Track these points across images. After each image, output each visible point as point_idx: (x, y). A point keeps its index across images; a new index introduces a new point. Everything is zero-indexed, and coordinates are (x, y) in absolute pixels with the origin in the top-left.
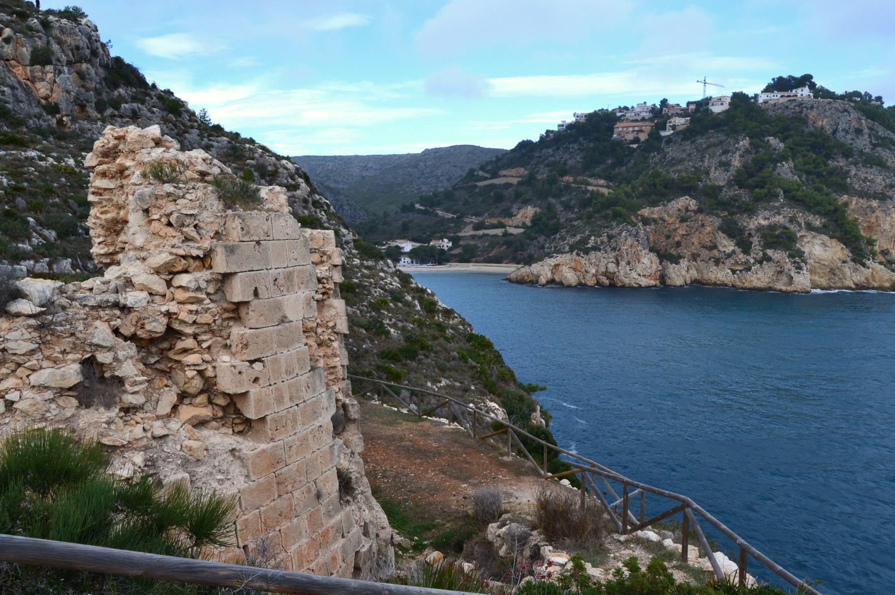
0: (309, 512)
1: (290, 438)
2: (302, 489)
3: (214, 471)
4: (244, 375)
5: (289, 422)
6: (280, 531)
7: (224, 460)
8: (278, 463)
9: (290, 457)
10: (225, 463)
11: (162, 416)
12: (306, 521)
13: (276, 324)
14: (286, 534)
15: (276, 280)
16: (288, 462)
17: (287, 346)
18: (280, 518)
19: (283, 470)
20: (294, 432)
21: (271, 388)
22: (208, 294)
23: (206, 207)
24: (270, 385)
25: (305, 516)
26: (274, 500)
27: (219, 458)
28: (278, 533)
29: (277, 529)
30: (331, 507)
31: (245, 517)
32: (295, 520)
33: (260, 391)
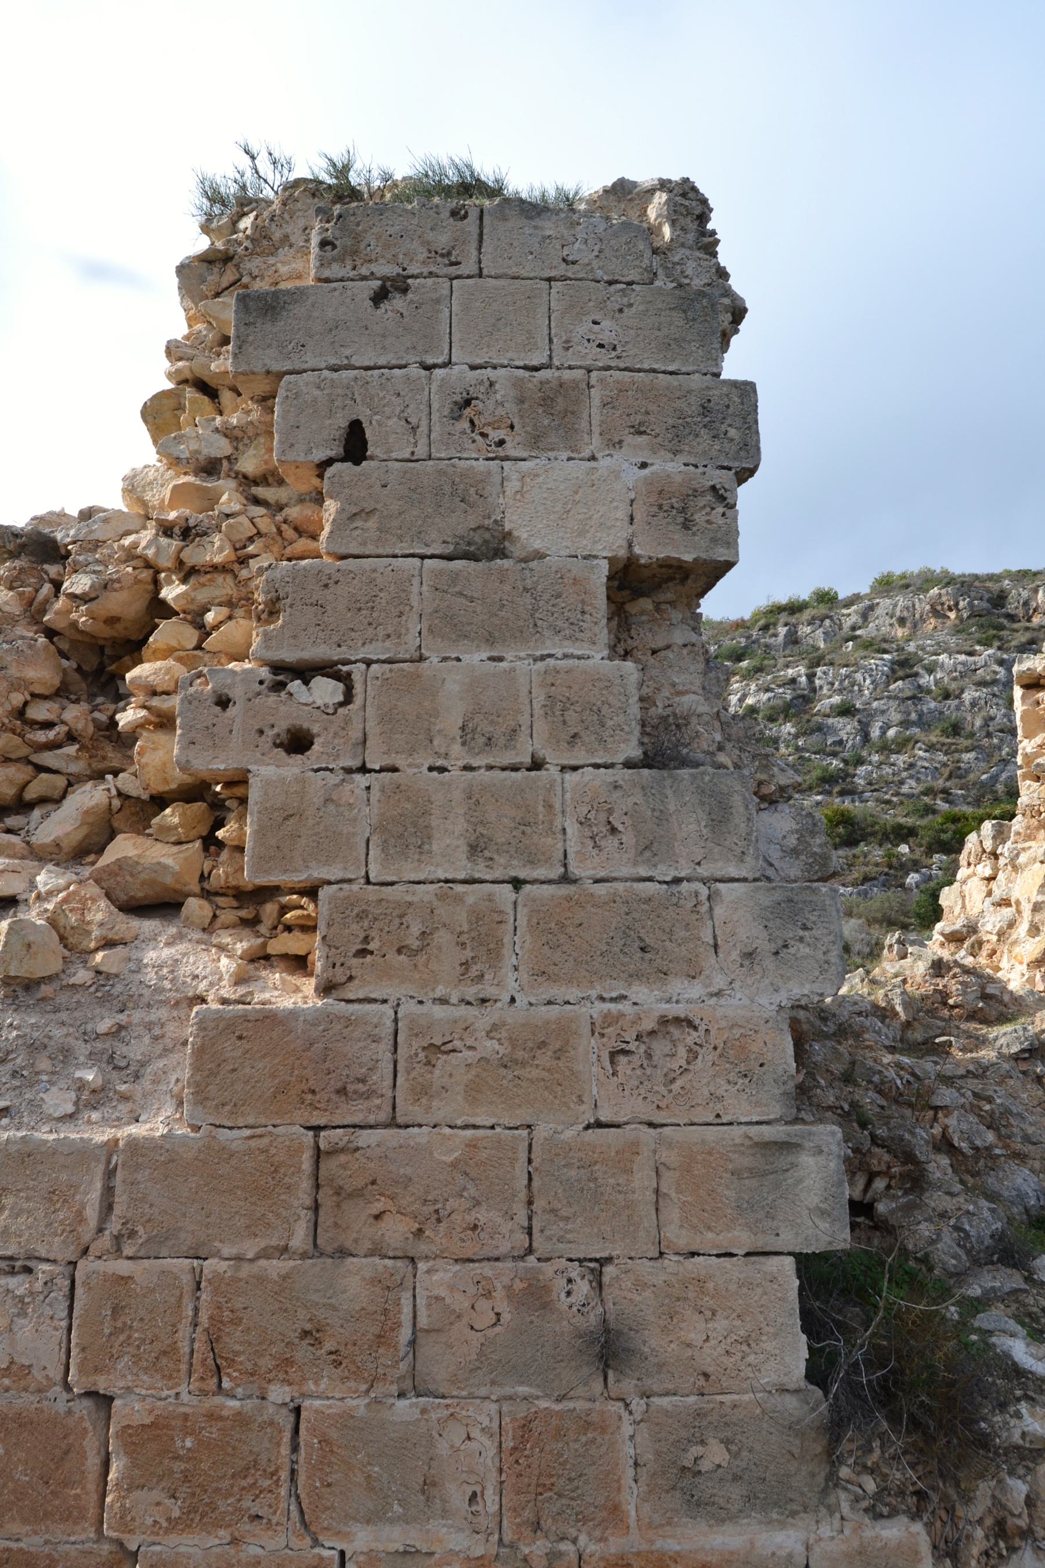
0: (522, 1411)
1: (439, 1012)
2: (487, 1269)
3: (82, 1050)
4: (232, 711)
5: (443, 937)
6: (297, 1411)
7: (149, 1026)
8: (342, 1091)
9: (422, 1092)
10: (147, 1040)
11: (43, 846)
12: (490, 1448)
13: (449, 549)
14: (324, 1441)
15: (467, 403)
16: (406, 1110)
17: (490, 640)
18: (303, 1352)
19: (366, 1138)
20: (471, 992)
21: (361, 780)
22: (246, 481)
23: (286, 237)
24: (363, 769)
25: (485, 1414)
26: (284, 1250)
27: (137, 1016)
28: (286, 1421)
29: (279, 1393)
30: (715, 1454)
31: (123, 1267)
32: (405, 1408)
33: (302, 781)
